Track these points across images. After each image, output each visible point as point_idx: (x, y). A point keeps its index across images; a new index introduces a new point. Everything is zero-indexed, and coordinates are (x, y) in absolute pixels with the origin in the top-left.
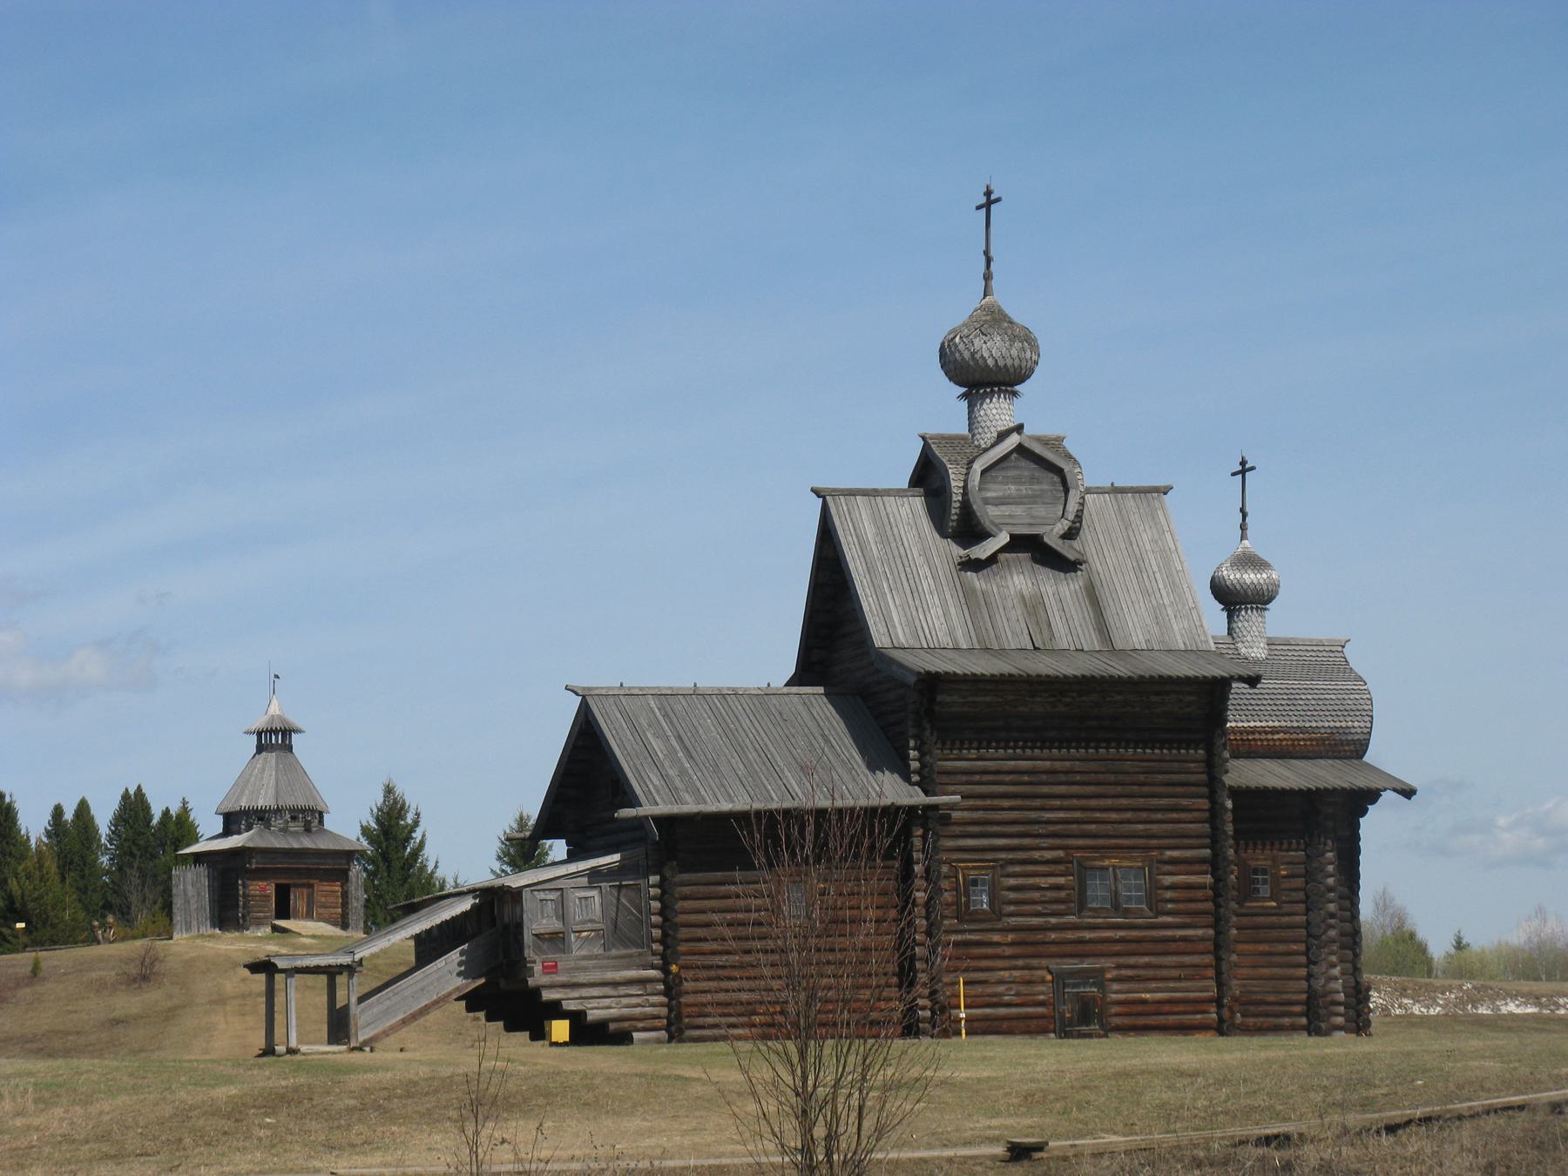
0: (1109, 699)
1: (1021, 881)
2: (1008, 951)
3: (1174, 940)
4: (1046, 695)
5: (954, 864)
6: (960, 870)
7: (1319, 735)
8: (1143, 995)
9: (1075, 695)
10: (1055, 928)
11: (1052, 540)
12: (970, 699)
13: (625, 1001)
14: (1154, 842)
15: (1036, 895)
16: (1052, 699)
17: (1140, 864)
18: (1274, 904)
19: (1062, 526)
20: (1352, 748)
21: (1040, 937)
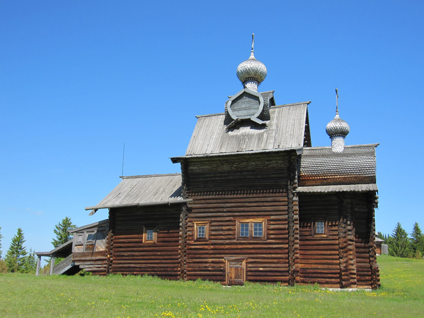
0: (250, 164)
1: (216, 228)
2: (211, 252)
3: (272, 248)
4: (227, 164)
5: (194, 222)
6: (195, 224)
7: (356, 175)
8: (260, 269)
9: (237, 163)
10: (227, 244)
11: (254, 119)
12: (201, 167)
13: (96, 266)
14: (267, 213)
15: (221, 232)
16: (229, 166)
17: (261, 221)
18: (325, 236)
19: (258, 114)
20: (372, 180)
21: (223, 247)
